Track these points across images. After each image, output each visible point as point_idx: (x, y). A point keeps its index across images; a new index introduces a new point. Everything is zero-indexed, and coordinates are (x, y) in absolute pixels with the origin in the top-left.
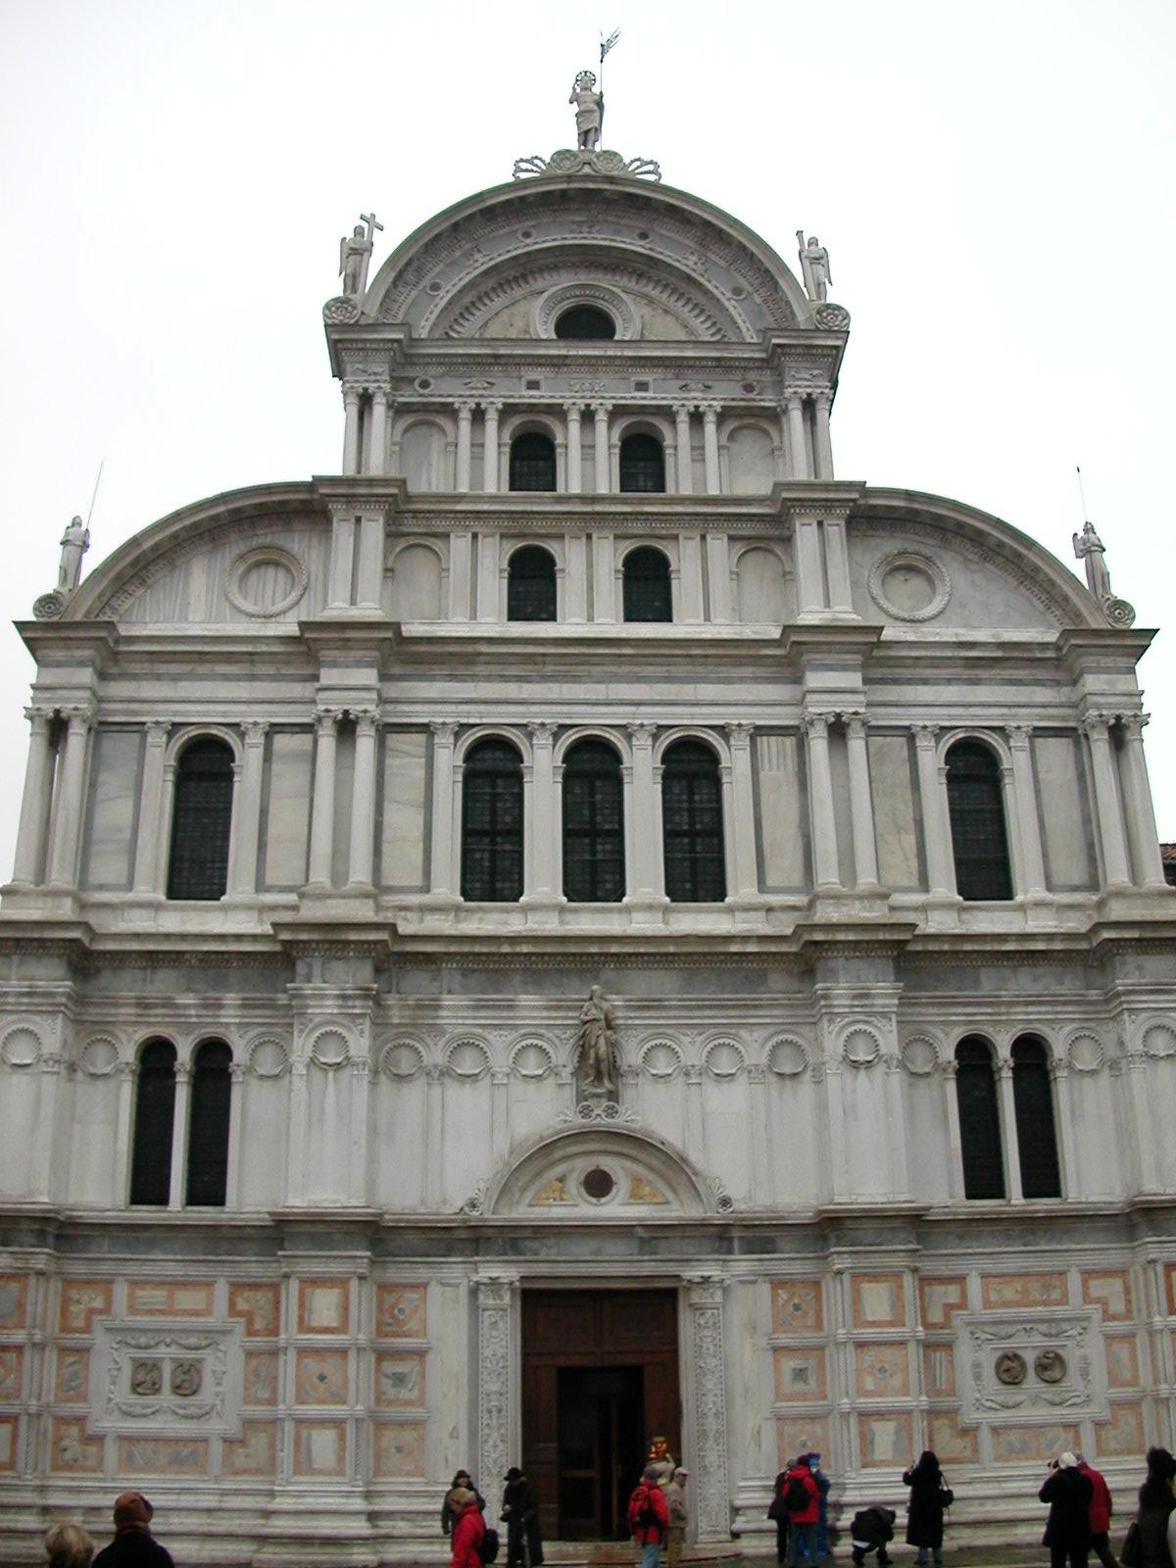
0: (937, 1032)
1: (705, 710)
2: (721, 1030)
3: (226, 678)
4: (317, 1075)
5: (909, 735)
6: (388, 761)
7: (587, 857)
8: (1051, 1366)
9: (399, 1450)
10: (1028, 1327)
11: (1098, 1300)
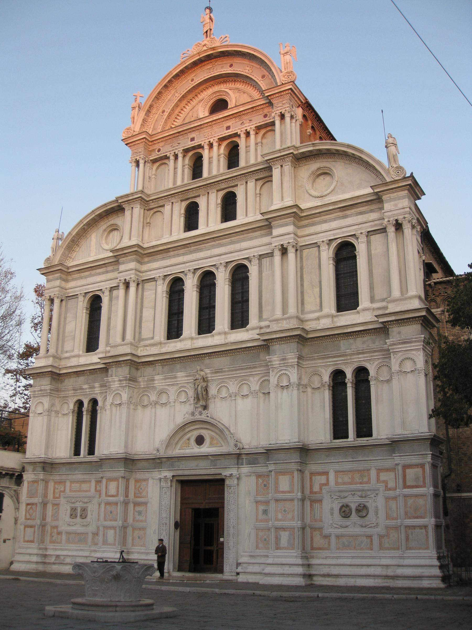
0: (323, 371)
1: (243, 252)
2: (242, 378)
3: (99, 274)
4: (114, 408)
5: (317, 245)
6: (145, 293)
7: (207, 317)
8: (362, 510)
9: (139, 537)
10: (353, 493)
11: (384, 482)
